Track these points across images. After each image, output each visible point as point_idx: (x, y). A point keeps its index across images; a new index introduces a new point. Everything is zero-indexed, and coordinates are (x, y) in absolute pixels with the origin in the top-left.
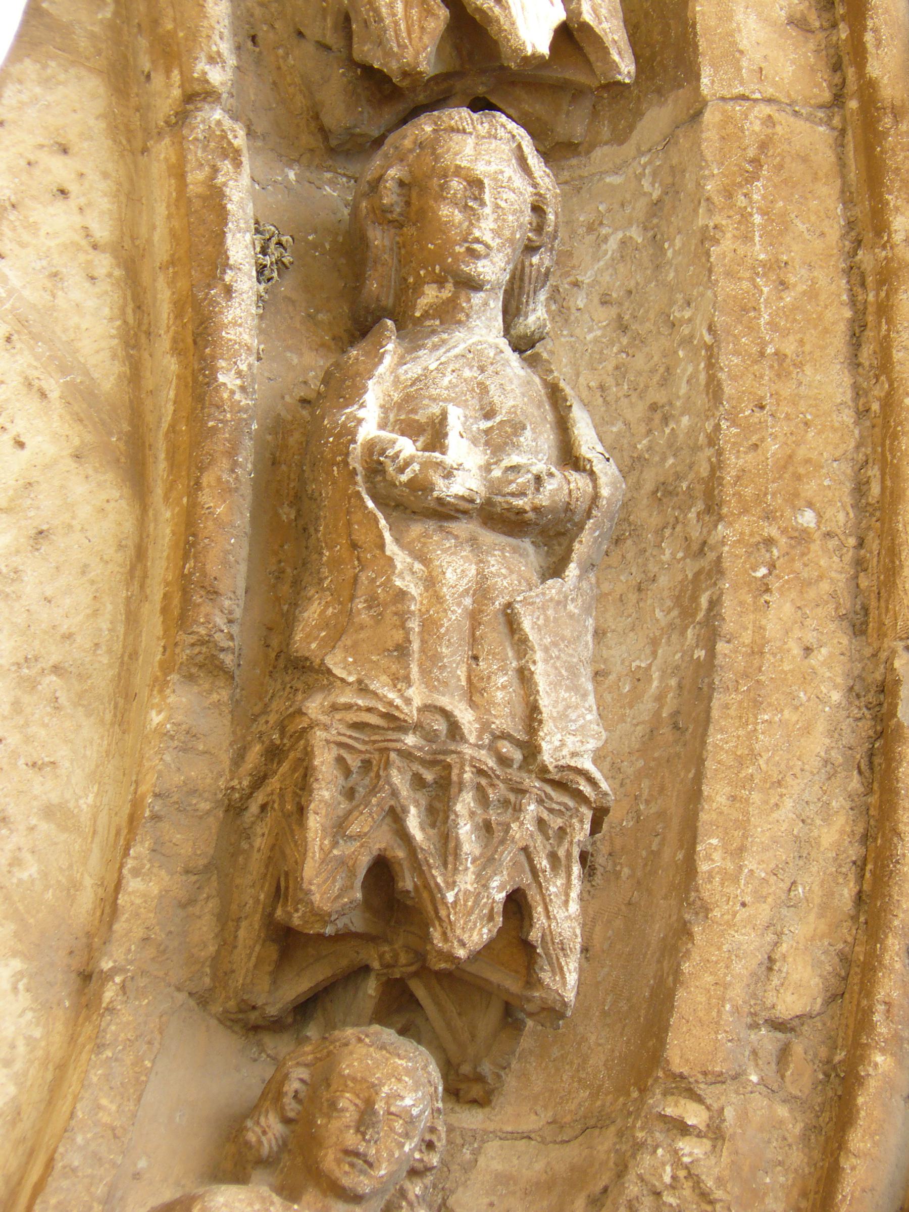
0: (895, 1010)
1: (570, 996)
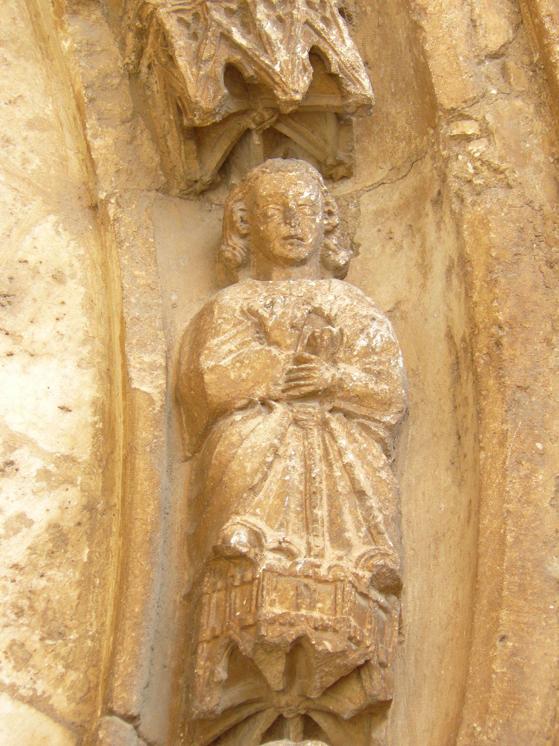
1: (370, 93)
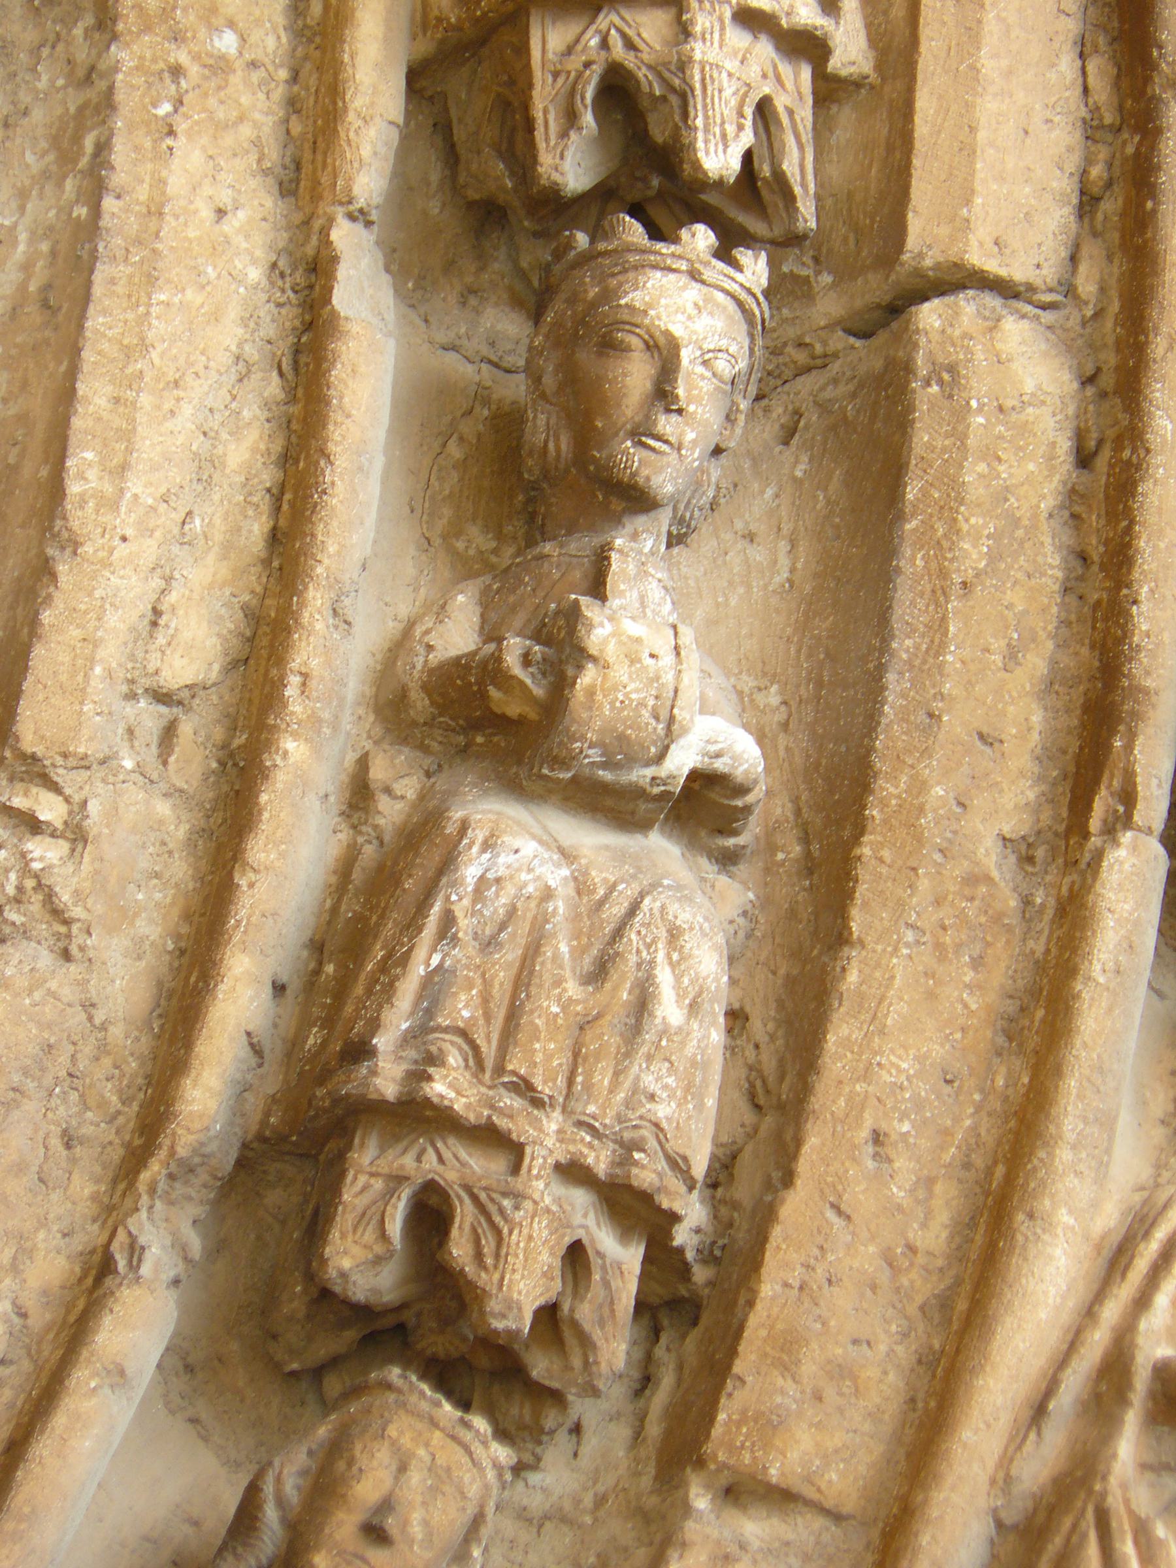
0: (313, 684)
